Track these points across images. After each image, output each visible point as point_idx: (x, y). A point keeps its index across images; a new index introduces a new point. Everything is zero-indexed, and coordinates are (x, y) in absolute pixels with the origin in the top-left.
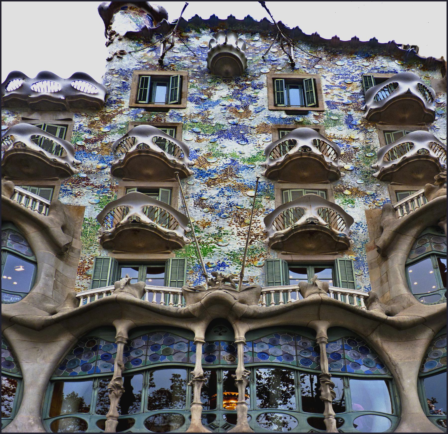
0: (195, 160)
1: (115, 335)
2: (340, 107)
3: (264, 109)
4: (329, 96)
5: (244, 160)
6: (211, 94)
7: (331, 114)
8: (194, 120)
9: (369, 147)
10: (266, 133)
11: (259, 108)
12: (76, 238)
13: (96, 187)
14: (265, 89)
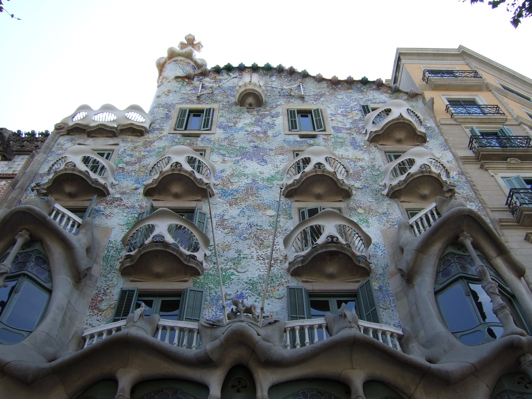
0: (220, 180)
1: (115, 394)
5: (263, 179)
6: (237, 122)
7: (337, 137)
8: (221, 143)
9: (374, 166)
10: (283, 155)
11: (276, 133)
12: (97, 264)
13: (127, 207)
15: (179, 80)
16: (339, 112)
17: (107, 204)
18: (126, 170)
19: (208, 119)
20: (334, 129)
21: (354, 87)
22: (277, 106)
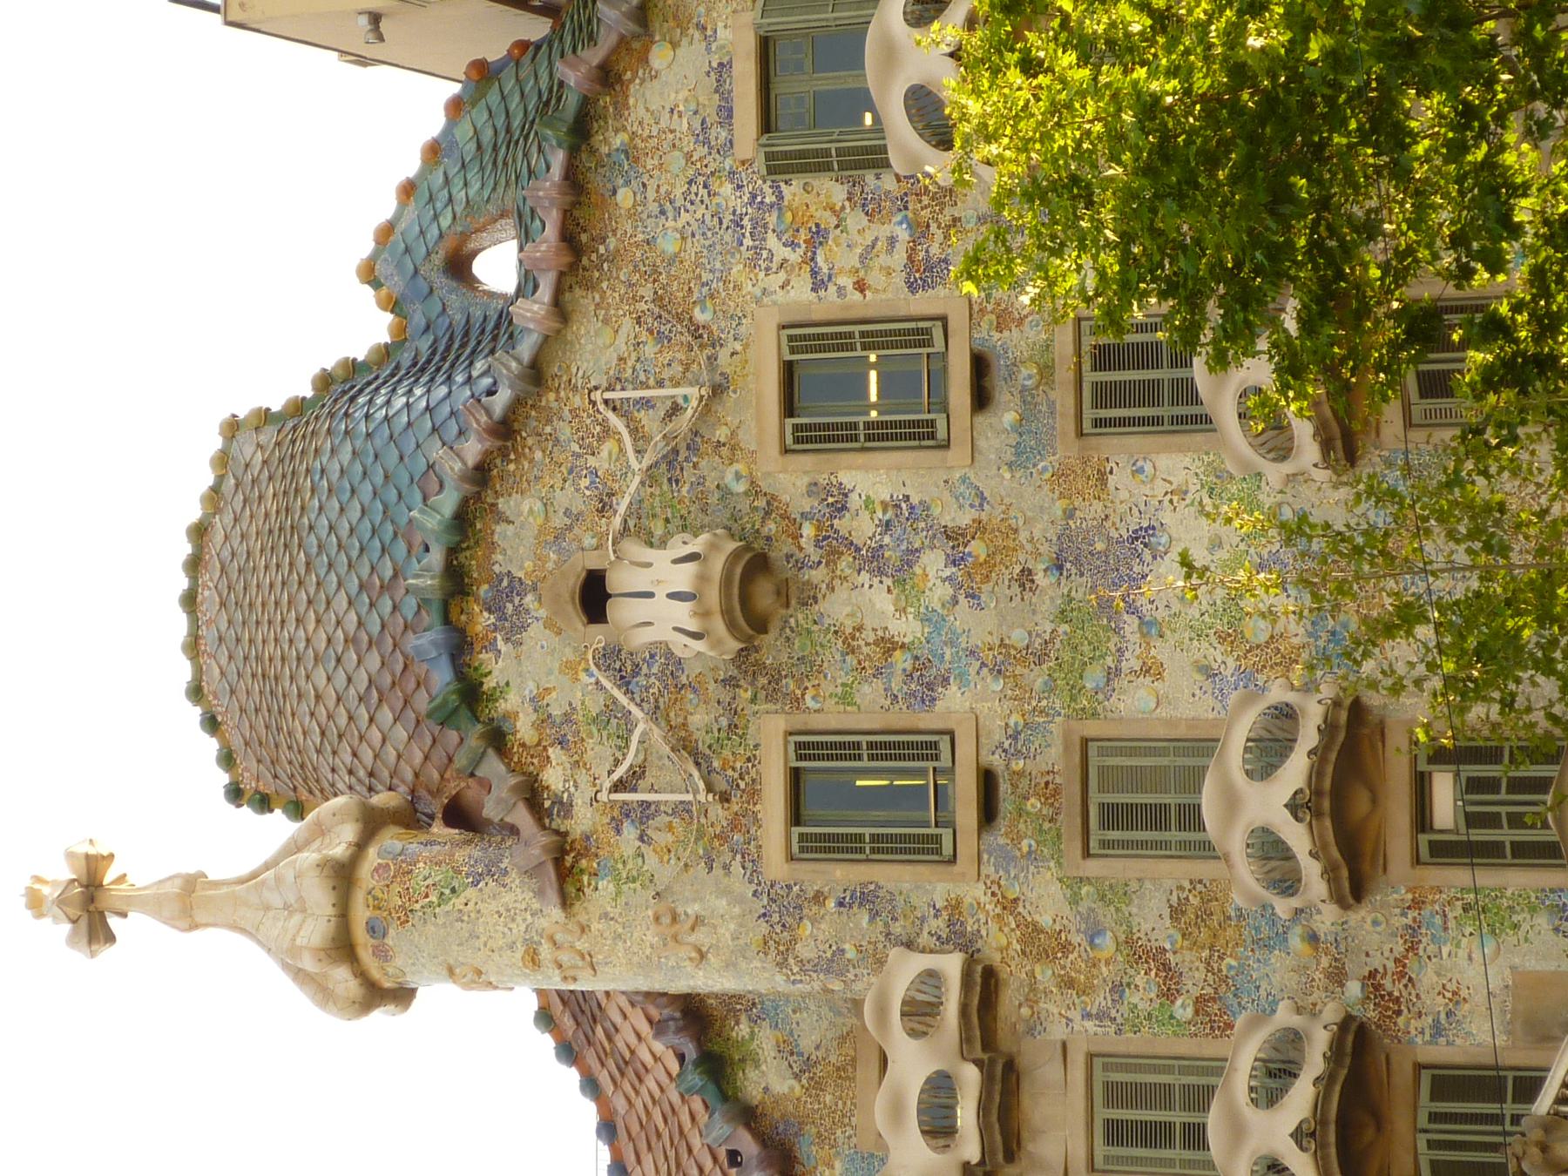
2: (935, 250)
3: (964, 479)
4: (875, 278)
8: (1039, 684)
14: (846, 478)
15: (571, 890)
16: (794, 257)
17: (1399, 1013)
18: (1209, 990)
19: (871, 745)
20: (926, 286)
21: (596, 182)
22: (755, 490)
